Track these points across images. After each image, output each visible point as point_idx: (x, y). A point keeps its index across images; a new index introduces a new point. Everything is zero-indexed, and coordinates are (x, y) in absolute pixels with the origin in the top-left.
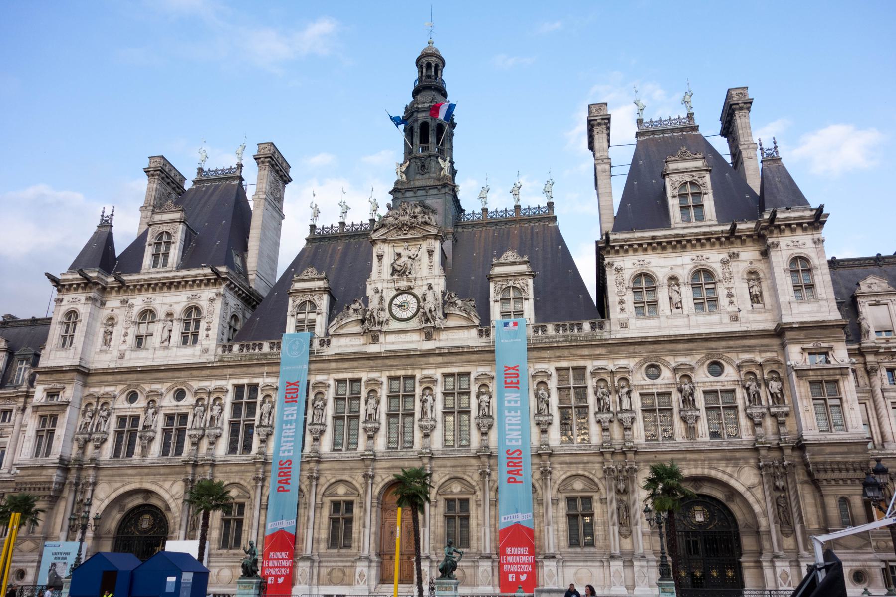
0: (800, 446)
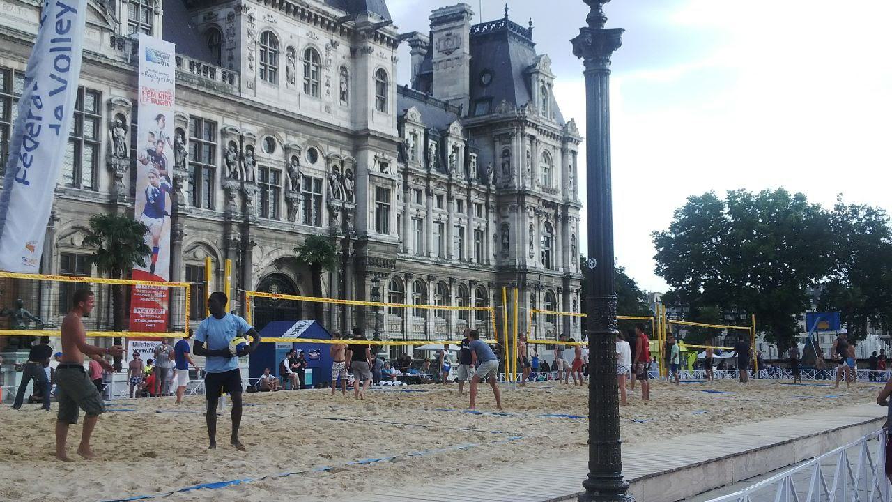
0: (363, 241)
